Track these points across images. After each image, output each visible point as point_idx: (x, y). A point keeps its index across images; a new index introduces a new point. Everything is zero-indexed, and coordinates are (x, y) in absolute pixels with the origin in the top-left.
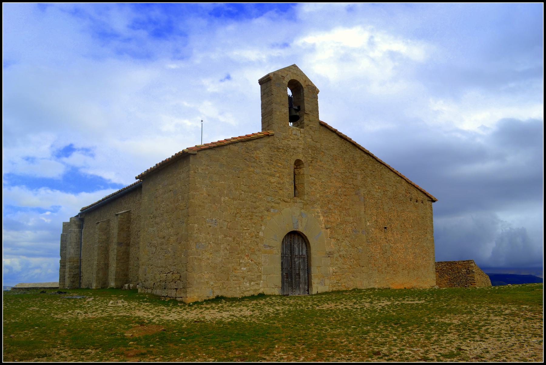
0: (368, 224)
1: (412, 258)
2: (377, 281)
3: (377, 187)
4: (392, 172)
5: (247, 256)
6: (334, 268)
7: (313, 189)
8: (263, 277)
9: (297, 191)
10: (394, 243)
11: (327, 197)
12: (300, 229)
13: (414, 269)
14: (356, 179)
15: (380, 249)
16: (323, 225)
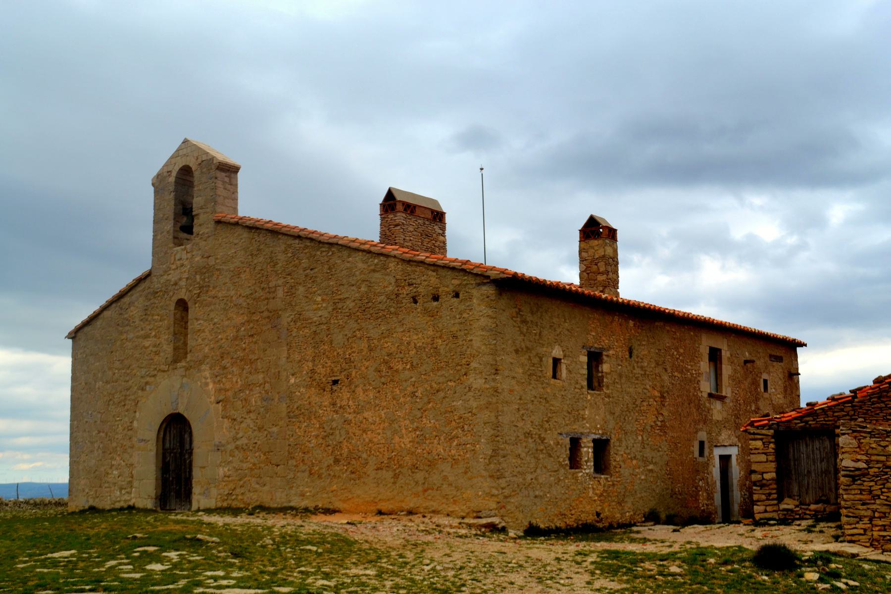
0: (292, 381)
1: (410, 442)
2: (308, 494)
3: (319, 299)
4: (360, 253)
5: (119, 455)
6: (226, 469)
7: (200, 340)
8: (136, 484)
9: (180, 352)
10: (354, 412)
11: (221, 347)
12: (181, 410)
13: (414, 468)
14: (273, 298)
15: (320, 428)
16: (213, 398)
